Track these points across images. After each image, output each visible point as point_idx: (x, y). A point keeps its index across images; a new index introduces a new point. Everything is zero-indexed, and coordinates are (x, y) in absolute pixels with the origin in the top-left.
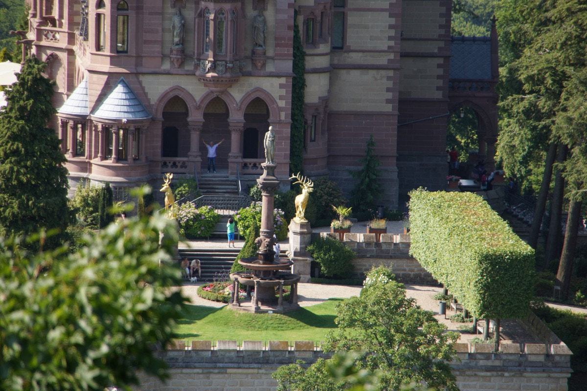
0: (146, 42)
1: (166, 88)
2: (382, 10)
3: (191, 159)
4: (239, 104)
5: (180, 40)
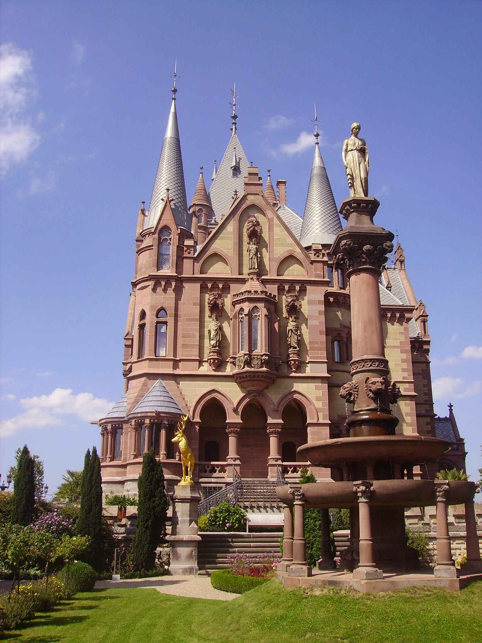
2: (395, 347)
4: (276, 405)
5: (216, 342)
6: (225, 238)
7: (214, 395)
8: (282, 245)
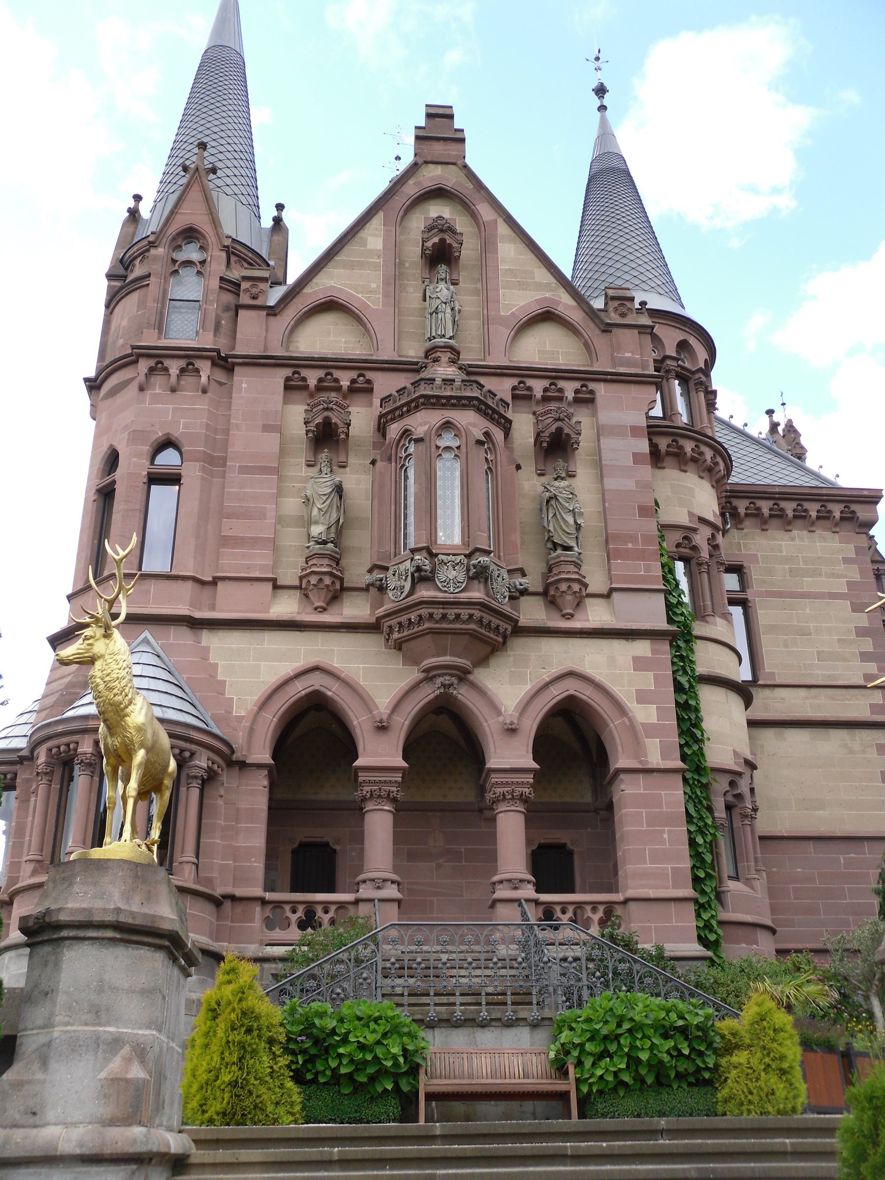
0: (226, 541)
1: (288, 668)
3: (365, 892)
6: (361, 265)
7: (316, 682)
8: (522, 286)
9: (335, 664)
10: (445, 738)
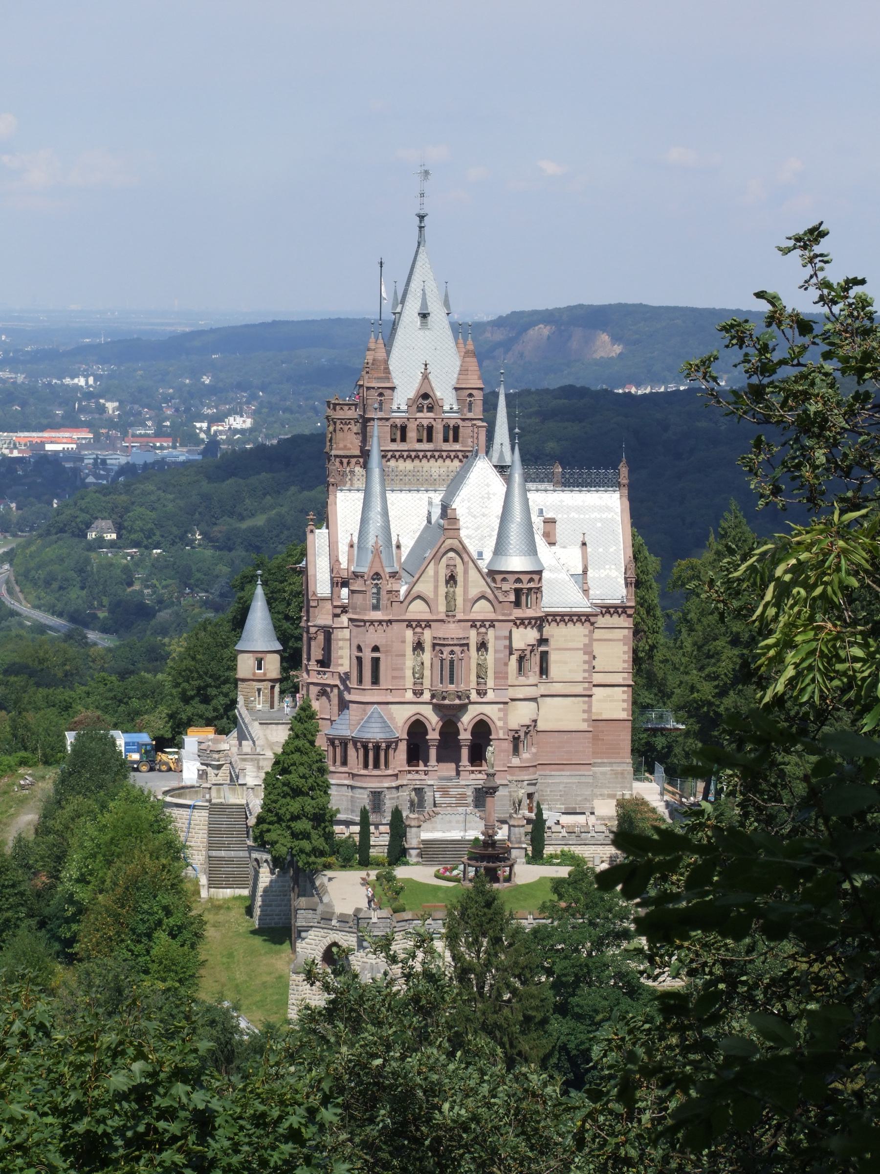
1: (410, 713)
9: (423, 712)
10: (449, 730)
